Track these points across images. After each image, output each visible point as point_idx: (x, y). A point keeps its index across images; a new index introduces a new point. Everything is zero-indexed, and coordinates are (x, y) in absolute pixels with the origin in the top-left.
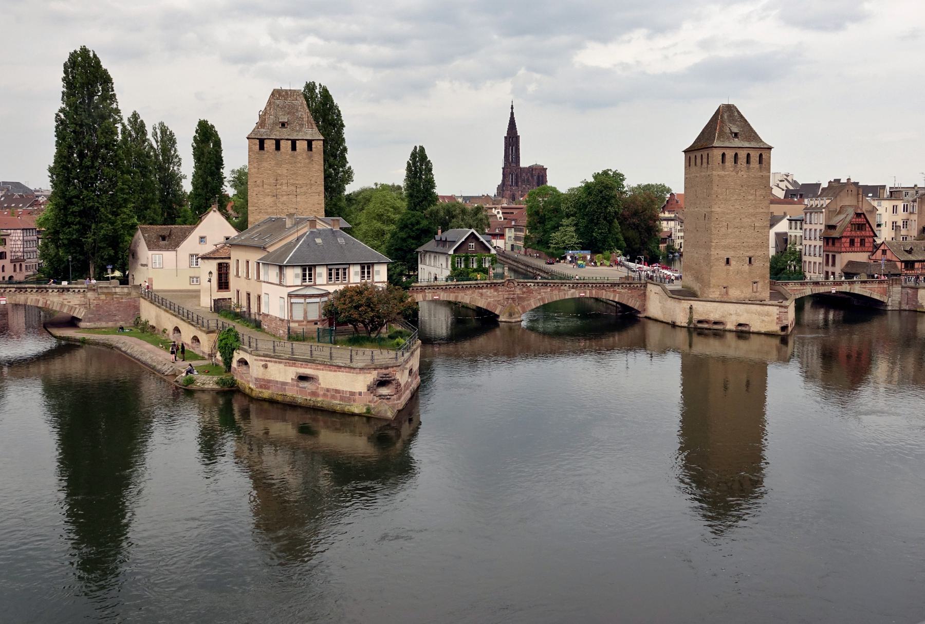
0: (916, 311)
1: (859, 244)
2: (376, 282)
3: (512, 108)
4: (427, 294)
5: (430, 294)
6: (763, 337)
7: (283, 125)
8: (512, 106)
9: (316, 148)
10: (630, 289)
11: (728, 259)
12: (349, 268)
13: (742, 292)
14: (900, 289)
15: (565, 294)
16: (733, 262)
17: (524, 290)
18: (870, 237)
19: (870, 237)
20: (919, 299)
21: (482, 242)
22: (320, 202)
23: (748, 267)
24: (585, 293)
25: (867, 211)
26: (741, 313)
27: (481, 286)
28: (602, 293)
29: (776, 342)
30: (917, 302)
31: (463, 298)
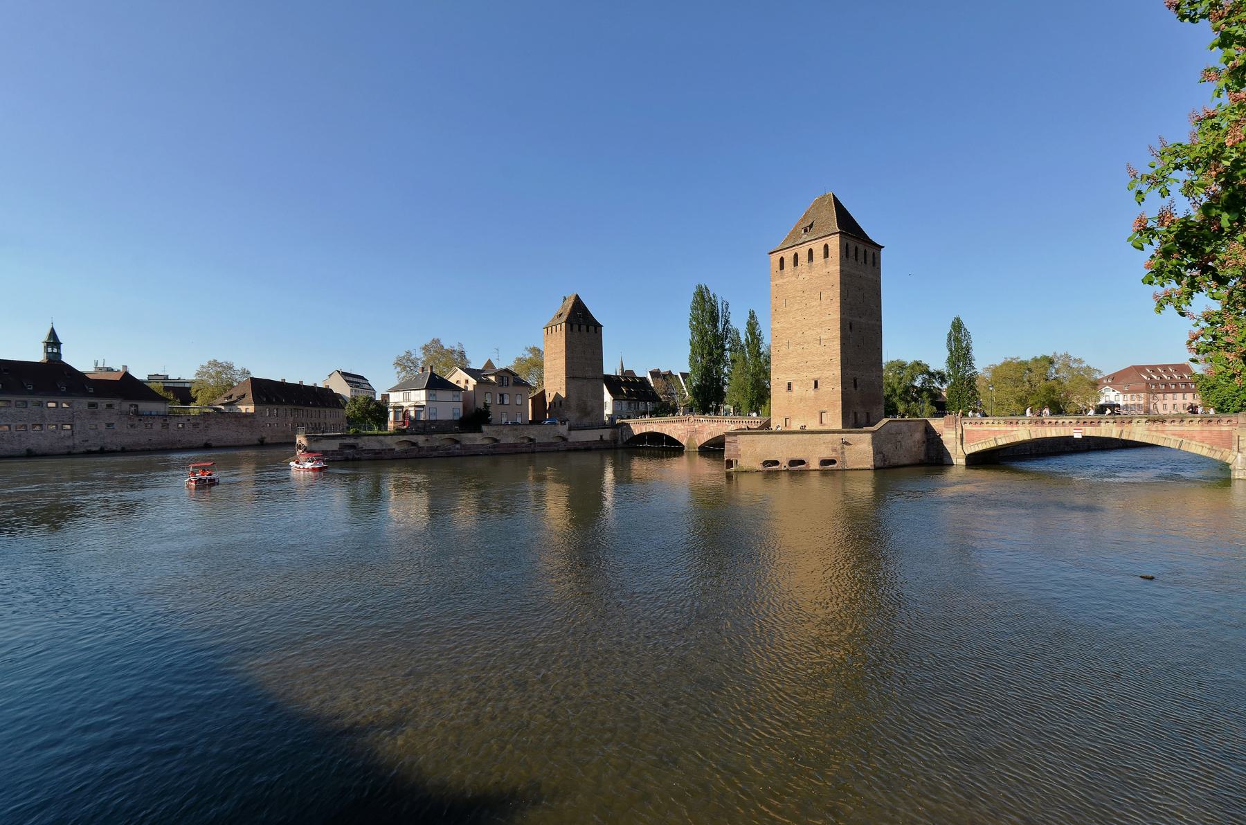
11: (789, 384)
16: (794, 387)
17: (700, 425)
23: (813, 392)
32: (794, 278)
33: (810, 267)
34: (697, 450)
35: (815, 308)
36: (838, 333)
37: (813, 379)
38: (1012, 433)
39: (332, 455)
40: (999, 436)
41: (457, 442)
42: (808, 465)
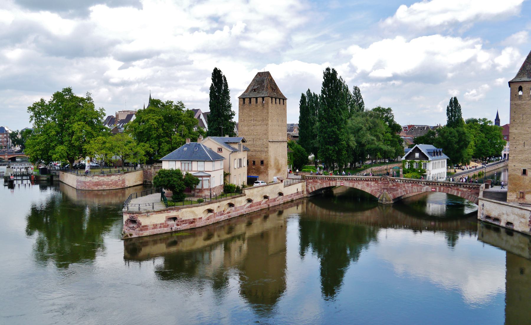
2: (205, 171)
4: (337, 182)
5: (339, 182)
6: (519, 235)
7: (255, 90)
9: (266, 101)
10: (469, 188)
12: (192, 163)
15: (421, 189)
17: (394, 184)
22: (267, 129)
26: (509, 214)
27: (367, 179)
28: (448, 190)
31: (357, 186)
39: (160, 227)
41: (231, 205)
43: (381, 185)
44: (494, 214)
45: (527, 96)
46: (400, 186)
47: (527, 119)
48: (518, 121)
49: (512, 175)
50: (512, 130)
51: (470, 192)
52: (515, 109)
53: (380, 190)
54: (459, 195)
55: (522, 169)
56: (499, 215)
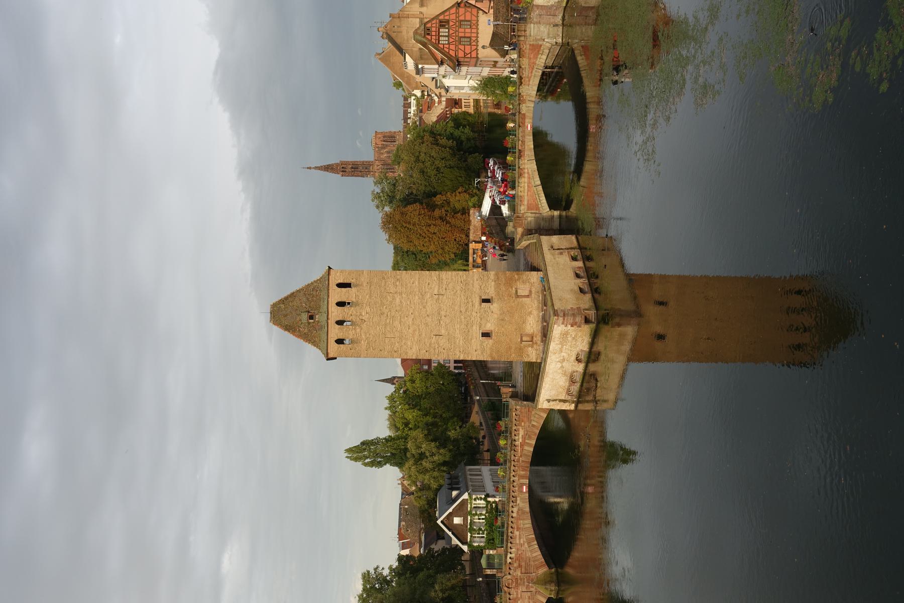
0: (565, 7)
1: (467, 30)
3: (310, 168)
8: (308, 168)
13: (530, 313)
14: (532, 25)
16: (488, 327)
17: (516, 565)
18: (457, 13)
19: (457, 13)
20: (549, 4)
21: (453, 510)
23: (495, 305)
24: (522, 485)
25: (422, 5)
26: (562, 358)
28: (523, 461)
29: (605, 329)
30: (552, 6)
32: (364, 326)
33: (356, 304)
34: (553, 570)
35: (403, 301)
36: (435, 274)
37: (481, 305)
38: (530, 173)
40: (533, 183)
42: (579, 268)
43: (519, 591)
44: (563, 382)
45: (354, 331)
46: (520, 553)
47: (394, 330)
48: (397, 344)
49: (491, 355)
50: (412, 354)
51: (525, 423)
52: (376, 352)
53: (529, 593)
54: (533, 442)
55: (481, 338)
56: (565, 374)
